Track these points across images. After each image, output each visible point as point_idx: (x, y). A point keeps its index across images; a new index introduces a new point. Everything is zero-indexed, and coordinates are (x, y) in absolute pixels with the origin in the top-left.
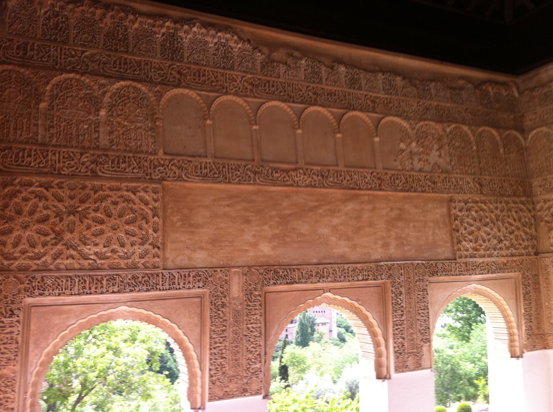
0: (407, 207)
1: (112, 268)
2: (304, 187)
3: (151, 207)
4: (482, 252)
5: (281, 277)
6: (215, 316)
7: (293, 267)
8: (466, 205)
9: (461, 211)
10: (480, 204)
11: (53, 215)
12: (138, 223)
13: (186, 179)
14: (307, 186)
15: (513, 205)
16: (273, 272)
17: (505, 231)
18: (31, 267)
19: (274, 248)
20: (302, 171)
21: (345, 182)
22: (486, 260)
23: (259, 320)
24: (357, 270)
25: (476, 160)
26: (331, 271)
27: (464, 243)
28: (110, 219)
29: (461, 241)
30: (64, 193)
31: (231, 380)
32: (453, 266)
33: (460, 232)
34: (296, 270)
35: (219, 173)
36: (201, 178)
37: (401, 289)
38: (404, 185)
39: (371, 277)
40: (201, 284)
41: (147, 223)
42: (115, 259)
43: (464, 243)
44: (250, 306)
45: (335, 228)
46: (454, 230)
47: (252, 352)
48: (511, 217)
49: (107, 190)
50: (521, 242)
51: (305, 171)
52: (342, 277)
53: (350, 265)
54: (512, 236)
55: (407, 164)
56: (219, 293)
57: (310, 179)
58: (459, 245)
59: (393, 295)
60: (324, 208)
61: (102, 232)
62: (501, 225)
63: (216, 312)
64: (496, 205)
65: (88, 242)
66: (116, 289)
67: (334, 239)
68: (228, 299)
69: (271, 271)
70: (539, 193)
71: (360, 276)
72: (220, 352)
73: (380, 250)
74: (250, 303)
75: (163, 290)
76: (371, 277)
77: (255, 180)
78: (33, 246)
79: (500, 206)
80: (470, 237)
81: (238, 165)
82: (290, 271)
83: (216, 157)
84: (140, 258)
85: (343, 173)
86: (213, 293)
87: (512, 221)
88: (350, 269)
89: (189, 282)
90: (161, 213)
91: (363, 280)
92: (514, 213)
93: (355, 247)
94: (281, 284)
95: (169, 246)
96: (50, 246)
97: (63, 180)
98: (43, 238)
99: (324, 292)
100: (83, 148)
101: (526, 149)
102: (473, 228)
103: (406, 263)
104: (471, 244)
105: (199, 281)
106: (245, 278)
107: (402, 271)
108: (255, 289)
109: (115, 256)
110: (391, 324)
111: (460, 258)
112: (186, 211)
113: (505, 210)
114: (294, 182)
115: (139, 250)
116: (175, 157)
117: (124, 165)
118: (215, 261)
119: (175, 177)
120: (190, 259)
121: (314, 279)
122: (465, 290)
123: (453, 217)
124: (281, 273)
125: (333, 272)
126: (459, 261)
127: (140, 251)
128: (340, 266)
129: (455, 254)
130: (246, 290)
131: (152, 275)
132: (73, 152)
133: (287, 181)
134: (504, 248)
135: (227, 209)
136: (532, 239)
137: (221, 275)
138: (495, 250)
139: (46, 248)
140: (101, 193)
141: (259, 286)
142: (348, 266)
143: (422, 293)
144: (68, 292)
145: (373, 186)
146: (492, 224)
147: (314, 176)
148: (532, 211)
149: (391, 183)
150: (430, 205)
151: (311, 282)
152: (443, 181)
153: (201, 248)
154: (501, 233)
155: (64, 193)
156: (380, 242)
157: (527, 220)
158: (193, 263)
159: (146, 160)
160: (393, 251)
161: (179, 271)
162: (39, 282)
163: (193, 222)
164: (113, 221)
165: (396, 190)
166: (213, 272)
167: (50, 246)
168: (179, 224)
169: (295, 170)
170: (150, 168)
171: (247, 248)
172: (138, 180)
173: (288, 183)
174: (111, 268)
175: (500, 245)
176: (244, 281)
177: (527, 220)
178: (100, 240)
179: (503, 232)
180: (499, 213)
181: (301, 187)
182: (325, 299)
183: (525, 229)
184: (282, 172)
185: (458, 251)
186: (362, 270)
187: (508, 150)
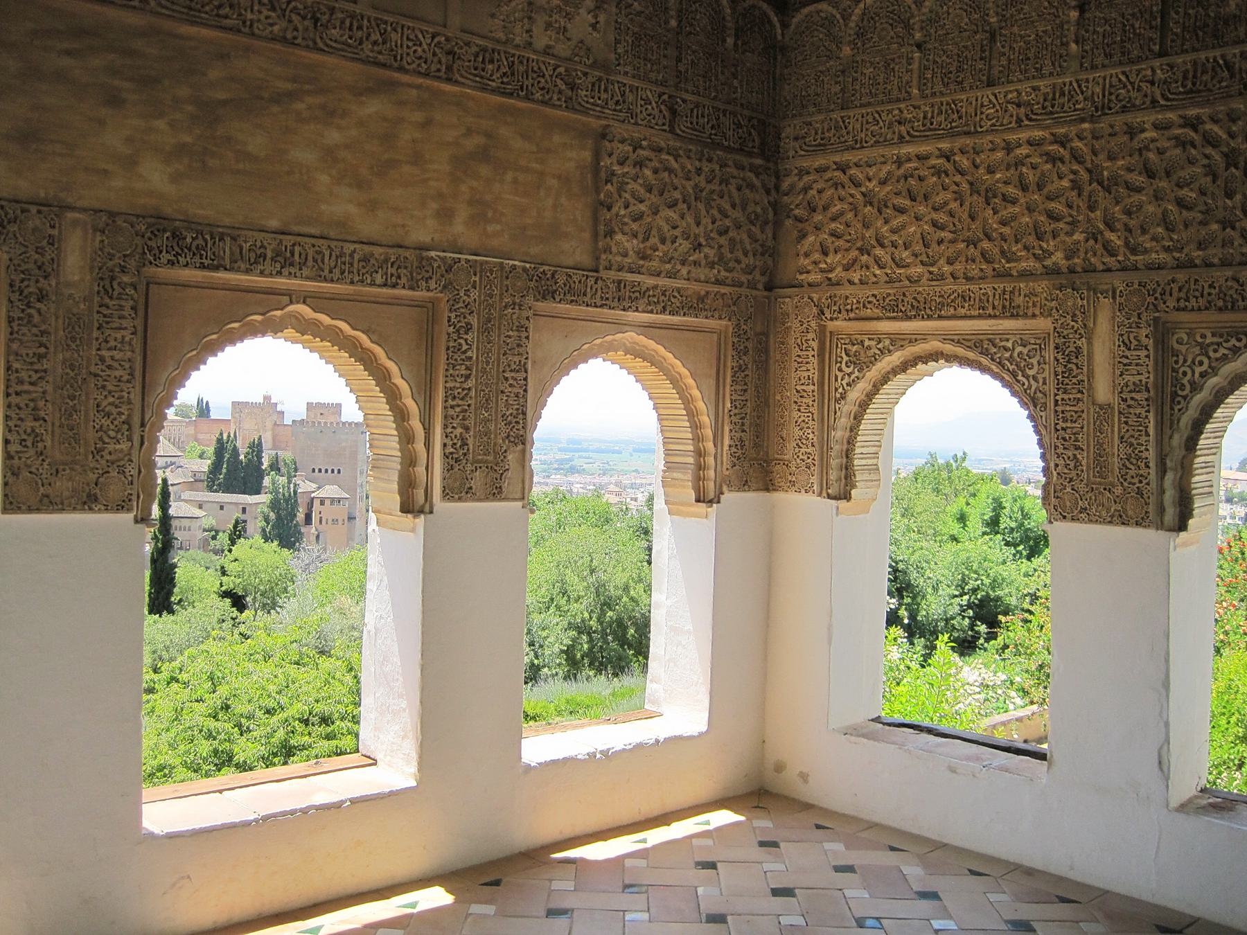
0: (504, 131)
2: (266, 39)
4: (655, 264)
5: (190, 250)
6: (19, 319)
9: (621, 164)
10: (664, 156)
15: (735, 172)
16: (168, 234)
17: (710, 227)
19: (175, 178)
21: (367, 46)
22: (663, 282)
24: (373, 261)
25: (672, 52)
26: (311, 253)
27: (619, 237)
33: (615, 210)
34: (228, 239)
38: (505, 80)
39: (404, 280)
43: (619, 237)
45: (329, 155)
46: (601, 204)
48: (726, 197)
50: (742, 257)
52: (337, 271)
53: (357, 246)
54: (723, 240)
55: (518, 30)
56: (31, 266)
60: (310, 100)
62: (703, 212)
63: (23, 311)
67: (324, 179)
68: (54, 284)
69: (165, 231)
70: (791, 153)
71: (379, 275)
73: (430, 222)
74: (107, 300)
79: (706, 168)
80: (635, 226)
85: (365, 21)
86: (16, 262)
87: (728, 207)
88: (356, 257)
91: (385, 285)
92: (734, 191)
93: (372, 206)
94: (187, 265)
99: (291, 302)
101: (783, 49)
102: (642, 207)
103: (487, 262)
104: (635, 241)
106: (98, 238)
108: (123, 270)
111: (606, 268)
113: (717, 181)
114: (244, 22)
118: (24, 187)
121: (267, 266)
122: (611, 342)
123: (603, 175)
124: (189, 240)
126: (604, 277)
128: (333, 244)
129: (598, 259)
133: (226, 17)
134: (703, 263)
135: (66, 62)
136: (763, 254)
137: (38, 222)
138: (683, 263)
141: (134, 264)
142: (352, 247)
143: (516, 333)
145: (433, 68)
146: (685, 206)
147: (294, 17)
148: (773, 192)
150: (557, 139)
151: (262, 273)
152: (593, 85)
154: (701, 228)
156: (435, 206)
157: (759, 210)
160: (459, 228)
165: (484, 89)
171: (109, 167)
173: (228, 22)
177: (759, 210)
180: (703, 184)
181: (259, 37)
182: (293, 320)
183: (753, 228)
186: (386, 261)
187: (744, 43)
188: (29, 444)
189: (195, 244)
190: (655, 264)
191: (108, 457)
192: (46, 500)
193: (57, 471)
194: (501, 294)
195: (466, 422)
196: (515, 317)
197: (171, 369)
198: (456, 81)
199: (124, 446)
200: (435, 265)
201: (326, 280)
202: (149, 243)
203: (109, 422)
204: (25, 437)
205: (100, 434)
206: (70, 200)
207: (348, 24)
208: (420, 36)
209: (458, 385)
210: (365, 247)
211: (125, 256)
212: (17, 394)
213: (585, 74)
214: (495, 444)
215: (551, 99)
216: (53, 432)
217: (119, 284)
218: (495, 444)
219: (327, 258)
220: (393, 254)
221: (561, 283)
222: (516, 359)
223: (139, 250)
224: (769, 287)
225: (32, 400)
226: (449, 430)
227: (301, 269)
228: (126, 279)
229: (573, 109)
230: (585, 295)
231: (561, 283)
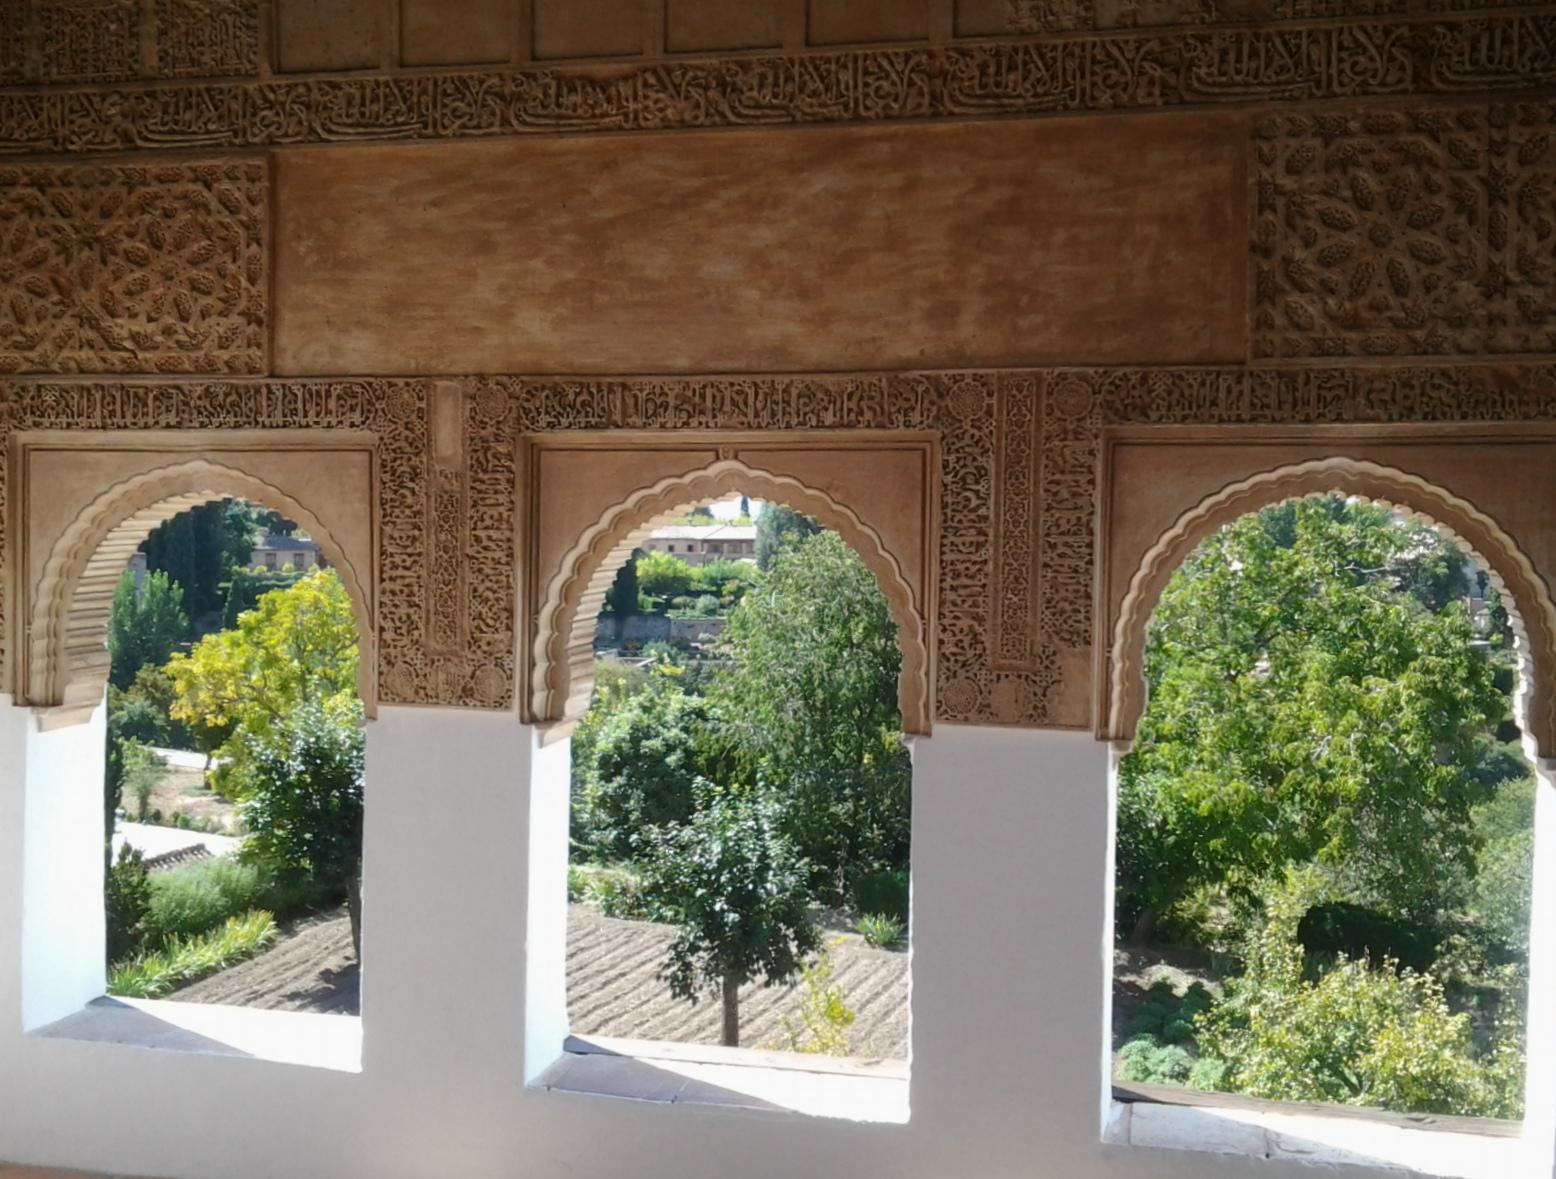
1: (165, 369)
3: (244, 218)
4: (1382, 334)
5: (572, 407)
7: (609, 379)
8: (1327, 145)
9: (1290, 170)
11: (52, 248)
12: (216, 261)
13: (325, 135)
14: (667, 126)
16: (546, 392)
17: (1533, 246)
18: (18, 364)
20: (652, 80)
23: (508, 522)
24: (820, 395)
27: (1294, 298)
28: (156, 252)
29: (1283, 291)
30: (72, 196)
31: (433, 661)
35: (410, 109)
36: (361, 130)
39: (868, 415)
40: (357, 418)
41: (234, 260)
42: (170, 348)
44: (483, 482)
45: (758, 262)
46: (1254, 248)
47: (487, 600)
49: (154, 183)
51: (663, 75)
53: (795, 377)
56: (403, 444)
57: (681, 104)
59: (949, 479)
60: (725, 194)
61: (144, 285)
63: (396, 492)
64: (1497, 136)
65: (120, 309)
66: (173, 421)
67: (752, 294)
68: (425, 459)
69: (543, 388)
72: (406, 590)
73: (918, 330)
74: (481, 475)
75: (271, 427)
76: (868, 415)
77: (505, 122)
78: (21, 321)
79: (1518, 135)
80: (1333, 275)
81: (463, 81)
82: (599, 385)
83: (402, 65)
84: (221, 347)
88: (794, 392)
89: (328, 412)
90: (265, 235)
91: (841, 426)
93: (825, 319)
94: (568, 427)
95: (287, 317)
96: (50, 320)
97: (70, 167)
98: (39, 303)
99: (718, 458)
100: (106, 81)
102: (1350, 239)
103: (1012, 374)
104: (1331, 302)
105: (352, 409)
106: (469, 406)
107: (994, 401)
108: (497, 438)
109: (171, 344)
110: (935, 569)
112: (329, 225)
114: (626, 115)
115: (218, 326)
116: (300, 79)
117: (188, 116)
118: (396, 360)
119: (298, 134)
120: (334, 350)
121: (670, 418)
124: (571, 397)
125: (736, 398)
127: (221, 330)
128: (759, 379)
130: (472, 439)
131: (247, 388)
132: (87, 96)
133: (603, 115)
135: (433, 214)
137: (406, 396)
138: (1458, 322)
139: (45, 323)
140: (142, 190)
141: (508, 430)
142: (786, 379)
143: (1069, 477)
144: (83, 421)
146: (1462, 220)
149: (983, 86)
151: (663, 426)
153: (362, 324)
155: (72, 196)
156: (922, 303)
158: (341, 362)
159: (235, 97)
160: (968, 331)
161: (305, 381)
162: (33, 398)
163: (343, 254)
164: (164, 260)
165: (1002, 113)
166: (385, 388)
167: (50, 320)
168: (314, 258)
169: (634, 76)
170: (244, 116)
171: (482, 324)
172: (216, 150)
174: (162, 371)
175: (1497, 306)
176: (467, 413)
178: (143, 306)
179: (1521, 249)
180: (1512, 168)
184: (589, 89)
188: (404, 631)
189: (580, 399)
191: (485, 648)
192: (422, 692)
193: (433, 661)
194: (1038, 422)
195: (980, 610)
196: (1067, 452)
197: (567, 548)
198: (951, 114)
199: (502, 635)
200: (920, 389)
201: (750, 427)
202: (526, 405)
203: (486, 609)
204: (398, 624)
205: (476, 623)
206: (441, 367)
207: (771, 79)
208: (885, 64)
209: (965, 557)
210: (808, 378)
211: (499, 423)
212: (392, 579)
213: (1204, 40)
214: (1032, 644)
215: (1133, 98)
216: (428, 619)
217: (494, 456)
218: (1032, 644)
219: (751, 401)
220: (847, 383)
221: (1160, 389)
223: (514, 414)
225: (408, 586)
226: (946, 622)
227: (714, 417)
228: (502, 448)
229: (1182, 102)
230: (1214, 403)
231: (1160, 389)
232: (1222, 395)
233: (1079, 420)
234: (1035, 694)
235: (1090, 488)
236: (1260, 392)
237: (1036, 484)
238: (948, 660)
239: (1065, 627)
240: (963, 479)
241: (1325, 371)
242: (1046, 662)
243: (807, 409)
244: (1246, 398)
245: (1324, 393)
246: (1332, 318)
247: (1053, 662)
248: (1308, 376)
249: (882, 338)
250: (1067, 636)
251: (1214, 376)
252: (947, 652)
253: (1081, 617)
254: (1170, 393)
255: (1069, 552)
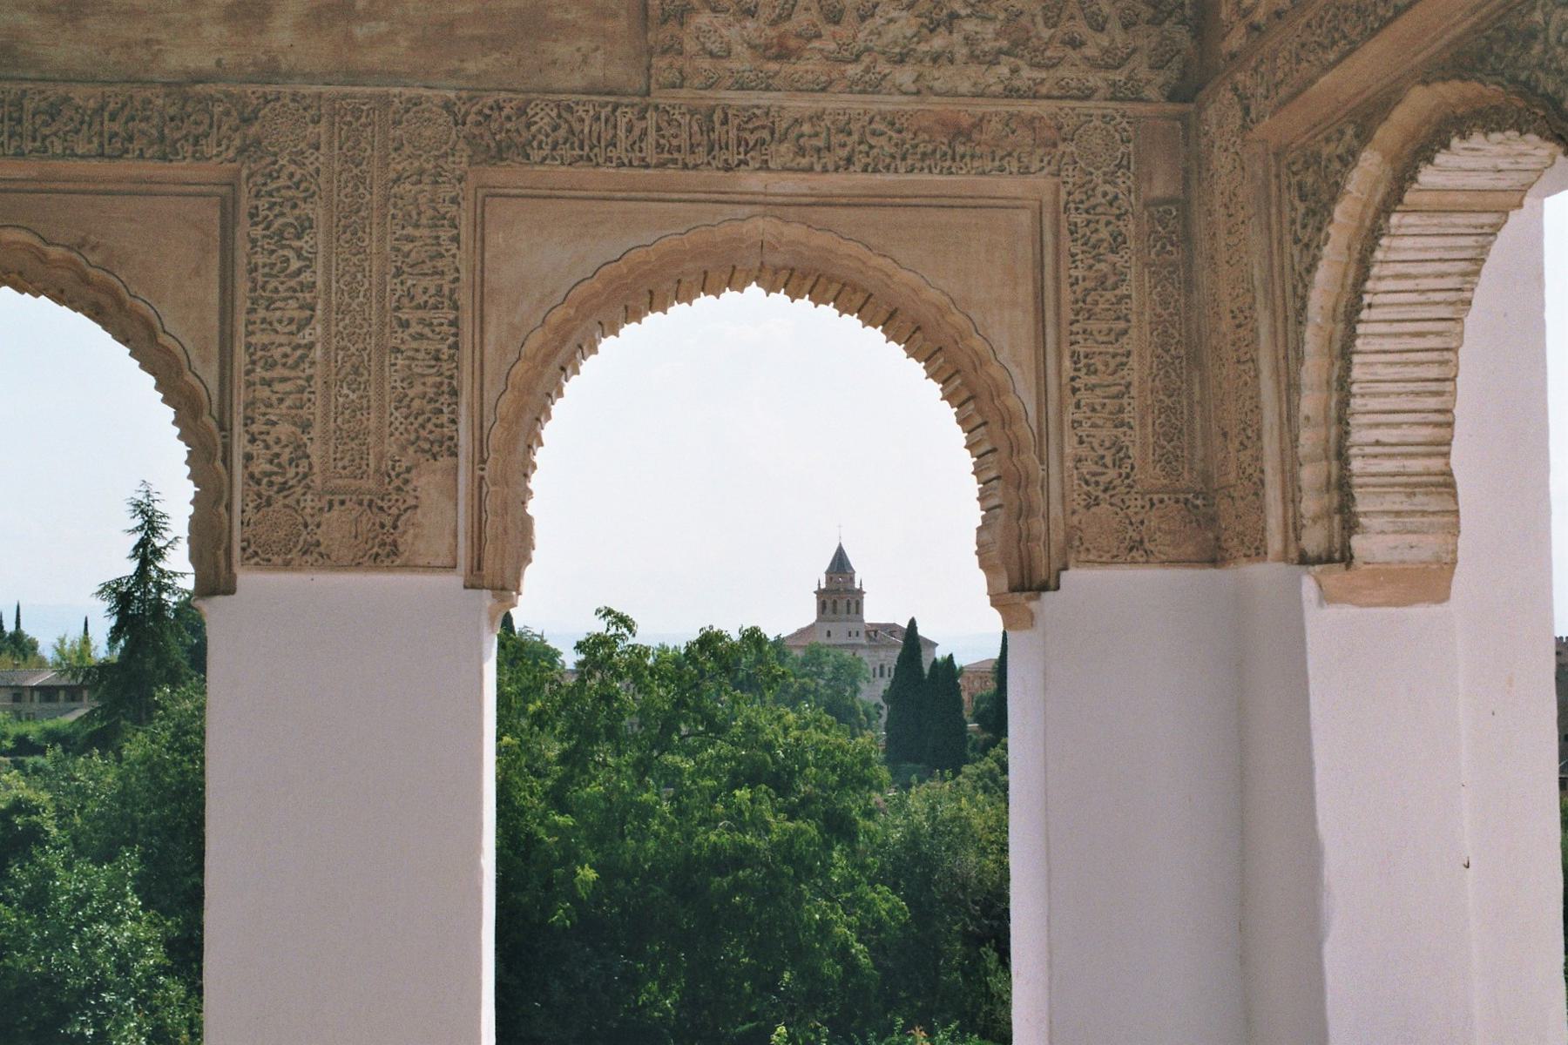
24: (67, 112)
27: (704, 19)
32: (622, 123)
37: (306, 209)
43: (704, 19)
50: (1081, 28)
58: (672, 28)
59: (258, 232)
73: (213, 32)
88: (29, 106)
91: (102, 155)
104: (750, 24)
107: (322, 127)
134: (962, 52)
138: (901, 60)
143: (426, 232)
175: (938, 43)
185: (664, 52)
190: (809, 66)
196: (422, 200)
200: (218, 109)
209: (283, 339)
218: (381, 457)
221: (543, 121)
222: (430, 283)
224: (1186, 91)
226: (254, 428)
231: (543, 121)
232: (622, 133)
233: (437, 158)
234: (382, 526)
235: (454, 247)
236: (668, 131)
237: (381, 240)
238: (258, 483)
239: (423, 433)
240: (280, 233)
241: (745, 109)
242: (397, 482)
243: (46, 131)
244: (652, 136)
245: (746, 135)
246: (752, 47)
247: (406, 482)
248: (726, 115)
249: (159, 42)
250: (426, 446)
251: (609, 108)
252: (257, 471)
253: (444, 418)
254: (555, 128)
255: (427, 331)
